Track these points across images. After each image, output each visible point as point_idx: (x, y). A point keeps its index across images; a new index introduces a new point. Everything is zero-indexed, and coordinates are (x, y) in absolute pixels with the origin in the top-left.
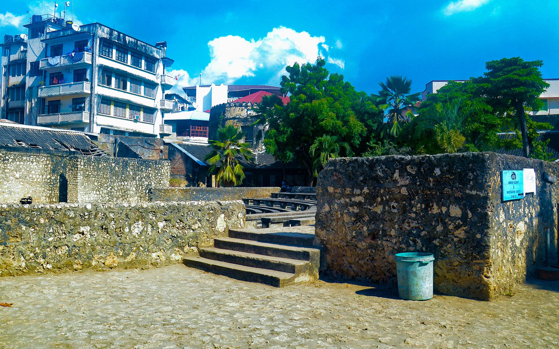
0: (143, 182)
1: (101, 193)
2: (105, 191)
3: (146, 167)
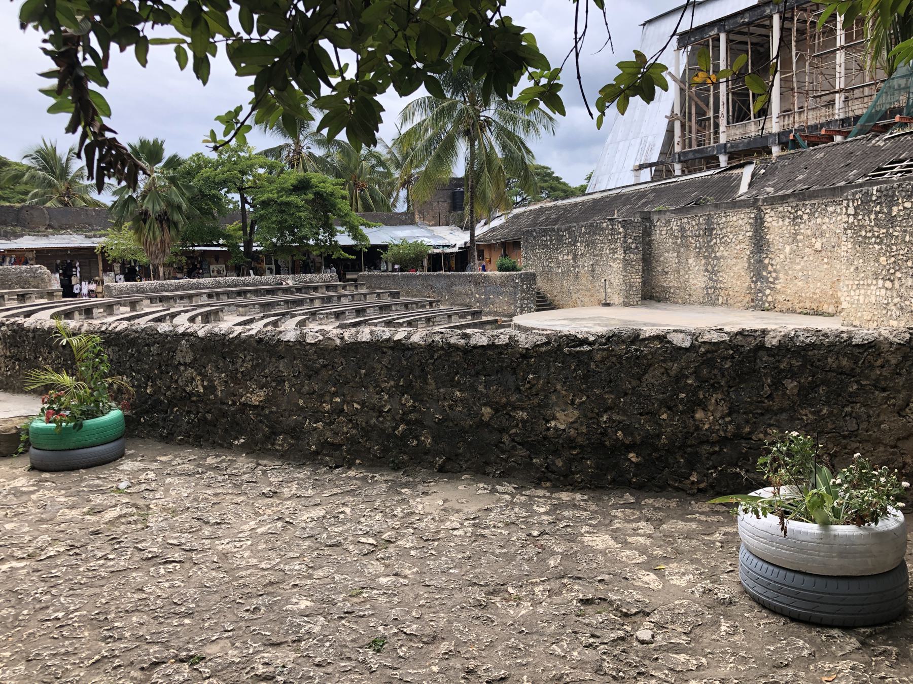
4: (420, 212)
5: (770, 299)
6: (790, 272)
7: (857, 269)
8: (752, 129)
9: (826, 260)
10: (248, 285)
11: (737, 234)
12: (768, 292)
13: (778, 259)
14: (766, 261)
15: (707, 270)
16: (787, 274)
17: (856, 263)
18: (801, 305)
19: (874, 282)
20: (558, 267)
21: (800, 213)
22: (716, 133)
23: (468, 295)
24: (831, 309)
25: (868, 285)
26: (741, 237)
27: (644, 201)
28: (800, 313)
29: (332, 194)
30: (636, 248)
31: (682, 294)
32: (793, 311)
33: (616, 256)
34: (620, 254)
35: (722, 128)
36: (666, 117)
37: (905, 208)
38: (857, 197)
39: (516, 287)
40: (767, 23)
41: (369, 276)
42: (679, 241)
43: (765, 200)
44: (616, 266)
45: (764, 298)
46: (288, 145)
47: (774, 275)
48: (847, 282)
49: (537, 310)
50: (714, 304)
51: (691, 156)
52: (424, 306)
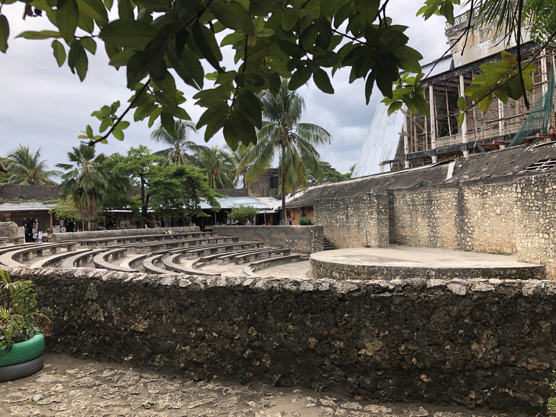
1: (551, 236)
4: (251, 189)
5: (470, 244)
6: (482, 227)
7: (525, 226)
8: (451, 141)
9: (503, 220)
10: (143, 234)
11: (447, 204)
12: (468, 239)
13: (474, 220)
14: (466, 220)
15: (429, 226)
16: (479, 228)
17: (524, 222)
18: (490, 248)
19: (537, 234)
20: (337, 223)
21: (486, 191)
22: (429, 143)
23: (281, 240)
24: (509, 251)
25: (533, 236)
26: (450, 205)
27: (388, 183)
28: (490, 253)
29: (198, 178)
30: (385, 211)
31: (414, 240)
32: (485, 252)
33: (373, 216)
34: (375, 215)
35: (433, 140)
36: (399, 133)
37: (553, 189)
38: (522, 182)
39: (311, 235)
40: (456, 80)
41: (219, 228)
42: (411, 207)
43: (464, 183)
44: (373, 222)
45: (466, 243)
46: (172, 149)
47: (472, 229)
48: (519, 234)
49: (324, 250)
50: (435, 247)
51: (414, 157)
52: (253, 247)
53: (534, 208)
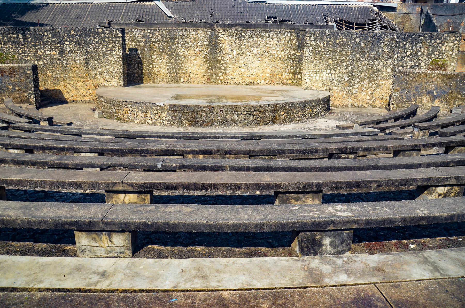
0: (406, 62)
1: (337, 72)
2: (344, 71)
3: (412, 42)
5: (222, 78)
14: (219, 58)
19: (325, 71)
33: (114, 53)
48: (309, 71)
53: (325, 53)
